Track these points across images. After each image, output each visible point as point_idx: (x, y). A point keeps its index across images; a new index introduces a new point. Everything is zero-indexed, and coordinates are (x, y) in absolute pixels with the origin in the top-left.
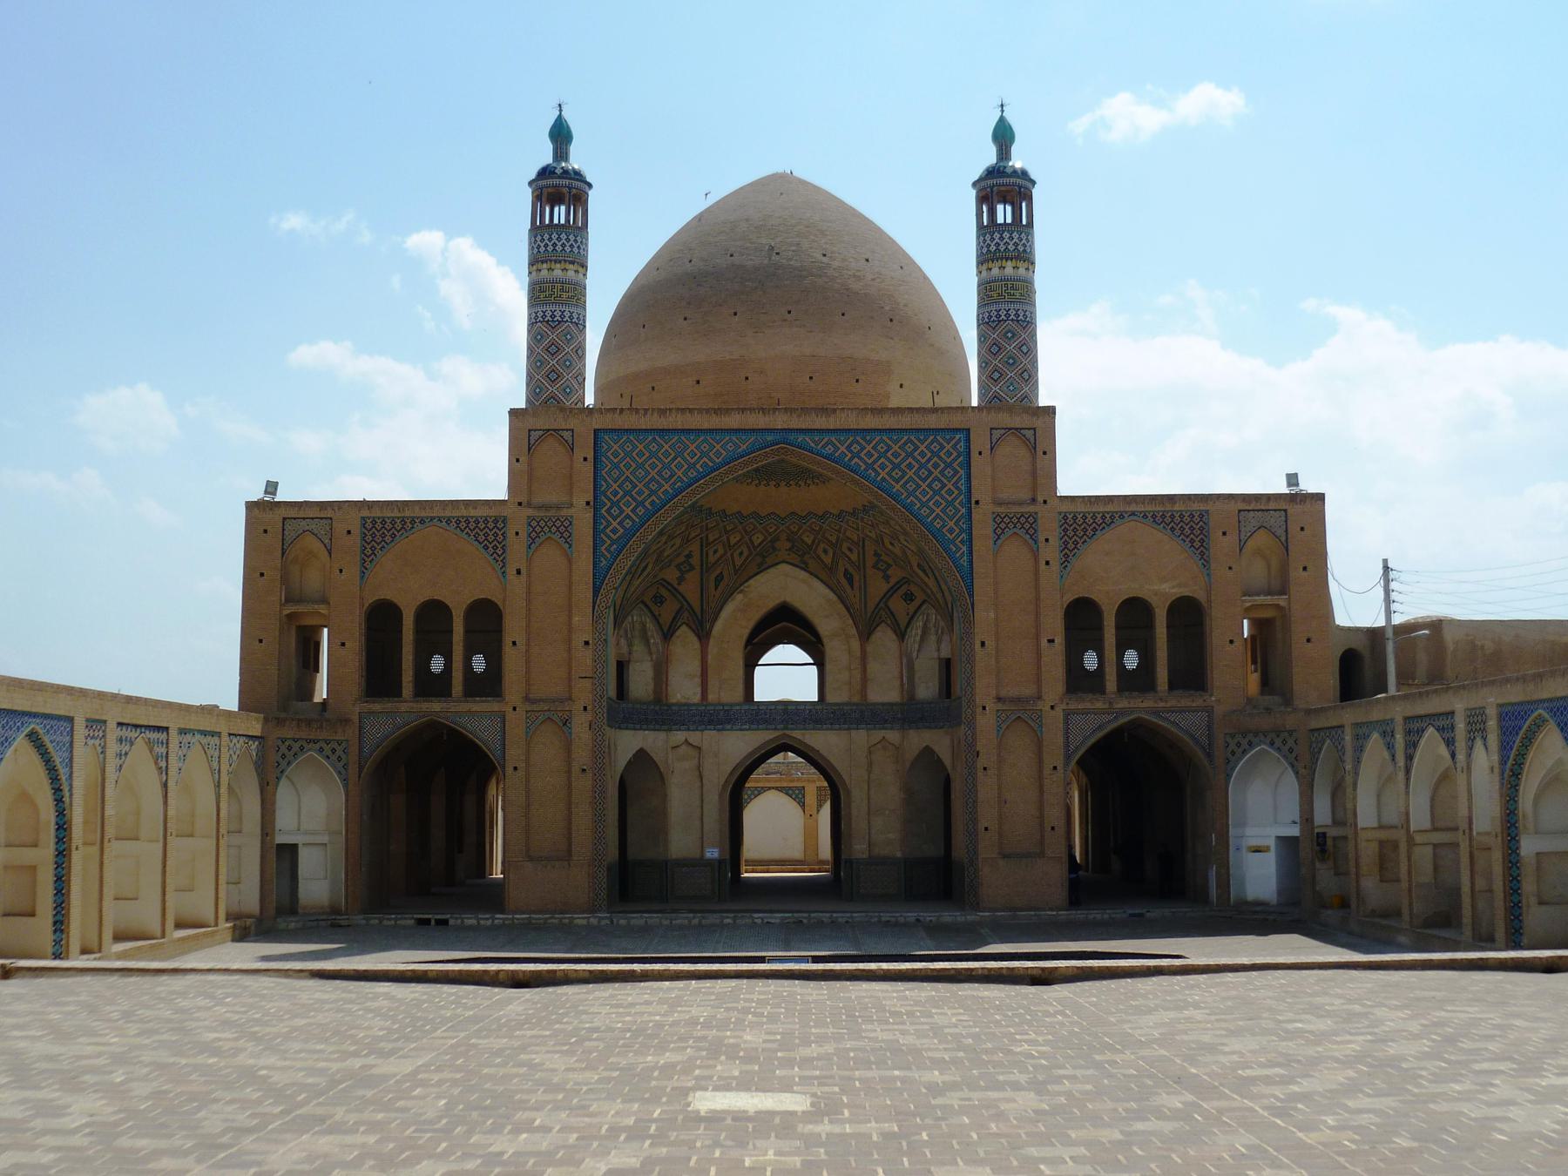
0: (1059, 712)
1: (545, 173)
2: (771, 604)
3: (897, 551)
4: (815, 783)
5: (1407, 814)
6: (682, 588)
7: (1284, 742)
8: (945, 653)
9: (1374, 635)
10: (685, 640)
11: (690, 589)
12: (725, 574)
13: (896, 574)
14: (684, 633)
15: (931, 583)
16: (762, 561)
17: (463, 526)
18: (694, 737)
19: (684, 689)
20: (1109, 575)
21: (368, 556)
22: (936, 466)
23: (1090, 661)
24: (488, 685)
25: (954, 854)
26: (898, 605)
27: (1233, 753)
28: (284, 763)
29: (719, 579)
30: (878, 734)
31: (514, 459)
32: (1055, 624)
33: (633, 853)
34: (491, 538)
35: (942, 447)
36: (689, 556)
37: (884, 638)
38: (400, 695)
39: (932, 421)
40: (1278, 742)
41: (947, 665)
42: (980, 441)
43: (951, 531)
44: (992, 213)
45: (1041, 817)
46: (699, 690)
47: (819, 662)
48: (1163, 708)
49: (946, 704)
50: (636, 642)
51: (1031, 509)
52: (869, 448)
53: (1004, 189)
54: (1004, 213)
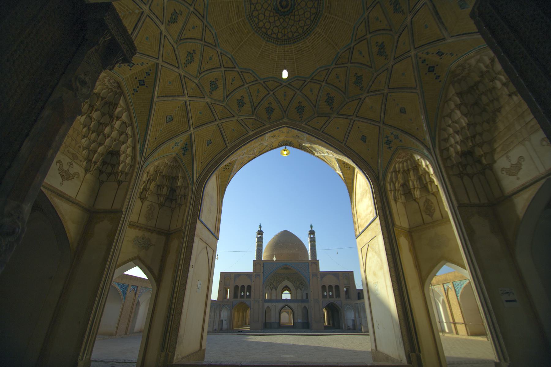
14: (274, 290)
18: (275, 304)
19: (274, 298)
20: (327, 282)
23: (325, 294)
24: (249, 297)
26: (300, 286)
31: (254, 267)
32: (320, 289)
37: (299, 290)
41: (307, 294)
42: (310, 264)
48: (335, 300)
49: (306, 300)
53: (312, 232)
54: (312, 236)
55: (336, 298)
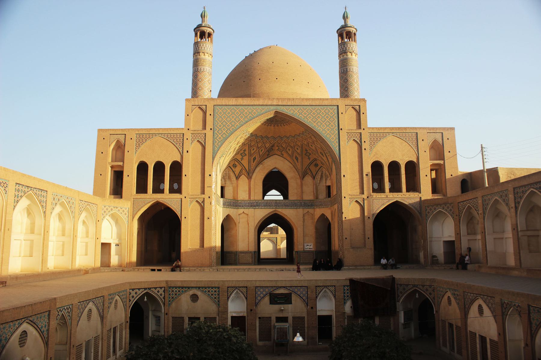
1: (199, 26)
3: (314, 148)
4: (282, 232)
5: (517, 224)
6: (242, 162)
7: (448, 208)
8: (329, 183)
10: (243, 179)
11: (245, 162)
12: (257, 157)
13: (312, 157)
14: (243, 178)
15: (325, 158)
16: (269, 153)
17: (169, 136)
18: (246, 211)
19: (243, 195)
21: (138, 146)
22: (327, 117)
24: (176, 189)
25: (333, 248)
26: (312, 168)
27: (429, 212)
28: (105, 214)
30: (306, 210)
32: (367, 169)
33: (226, 249)
34: (178, 140)
35: (329, 111)
36: (245, 151)
37: (308, 179)
38: (146, 193)
39: (326, 103)
40: (446, 208)
43: (333, 139)
45: (365, 235)
46: (248, 196)
50: (227, 180)
52: (305, 111)
55: (408, 191)
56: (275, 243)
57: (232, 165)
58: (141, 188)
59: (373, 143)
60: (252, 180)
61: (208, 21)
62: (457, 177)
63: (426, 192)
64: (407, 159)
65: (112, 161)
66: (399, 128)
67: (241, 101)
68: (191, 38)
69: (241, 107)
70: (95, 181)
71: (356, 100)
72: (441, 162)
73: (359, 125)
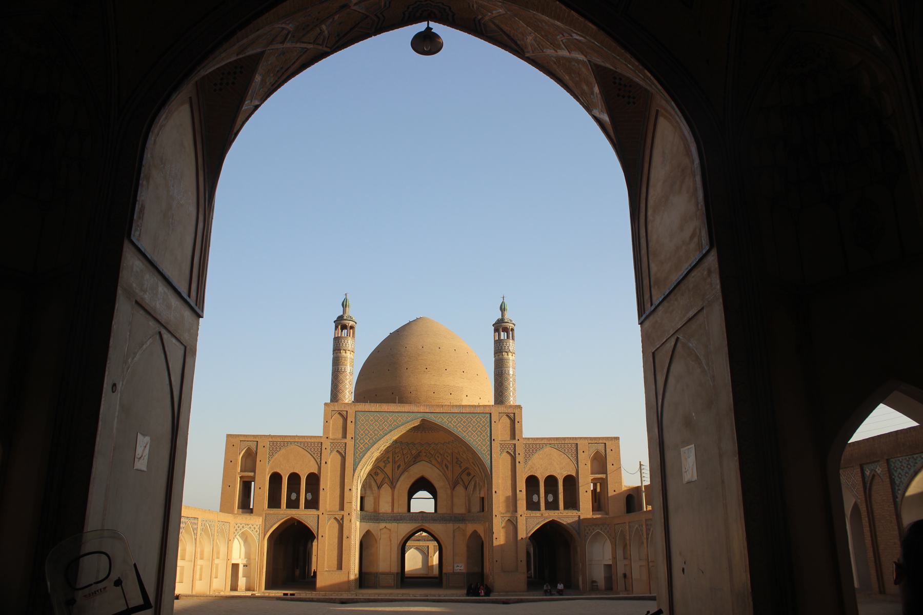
0: (524, 518)
1: (340, 318)
2: (418, 476)
4: (433, 545)
9: (637, 489)
10: (386, 491)
11: (388, 470)
14: (386, 489)
15: (477, 469)
16: (416, 459)
18: (388, 525)
19: (385, 507)
23: (535, 498)
24: (313, 504)
26: (464, 477)
29: (399, 467)
30: (457, 525)
32: (522, 485)
33: (363, 570)
37: (460, 489)
39: (478, 410)
44: (499, 335)
47: (435, 497)
51: (514, 442)
54: (503, 335)
55: (566, 508)
56: (426, 556)
57: (372, 475)
58: (274, 502)
59: (527, 458)
60: (396, 490)
61: (350, 312)
62: (621, 493)
63: (586, 509)
64: (565, 474)
65: (241, 471)
66: (557, 439)
67: (385, 407)
68: (330, 332)
69: (385, 414)
70: (222, 494)
71: (511, 406)
72: (603, 476)
73: (513, 435)
